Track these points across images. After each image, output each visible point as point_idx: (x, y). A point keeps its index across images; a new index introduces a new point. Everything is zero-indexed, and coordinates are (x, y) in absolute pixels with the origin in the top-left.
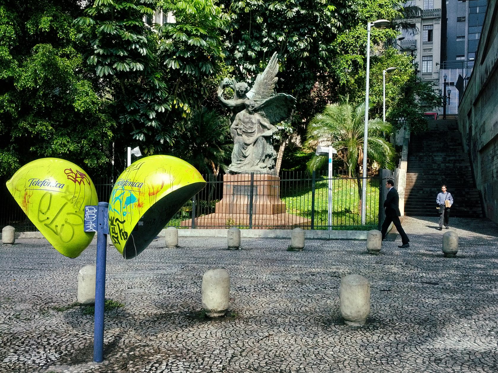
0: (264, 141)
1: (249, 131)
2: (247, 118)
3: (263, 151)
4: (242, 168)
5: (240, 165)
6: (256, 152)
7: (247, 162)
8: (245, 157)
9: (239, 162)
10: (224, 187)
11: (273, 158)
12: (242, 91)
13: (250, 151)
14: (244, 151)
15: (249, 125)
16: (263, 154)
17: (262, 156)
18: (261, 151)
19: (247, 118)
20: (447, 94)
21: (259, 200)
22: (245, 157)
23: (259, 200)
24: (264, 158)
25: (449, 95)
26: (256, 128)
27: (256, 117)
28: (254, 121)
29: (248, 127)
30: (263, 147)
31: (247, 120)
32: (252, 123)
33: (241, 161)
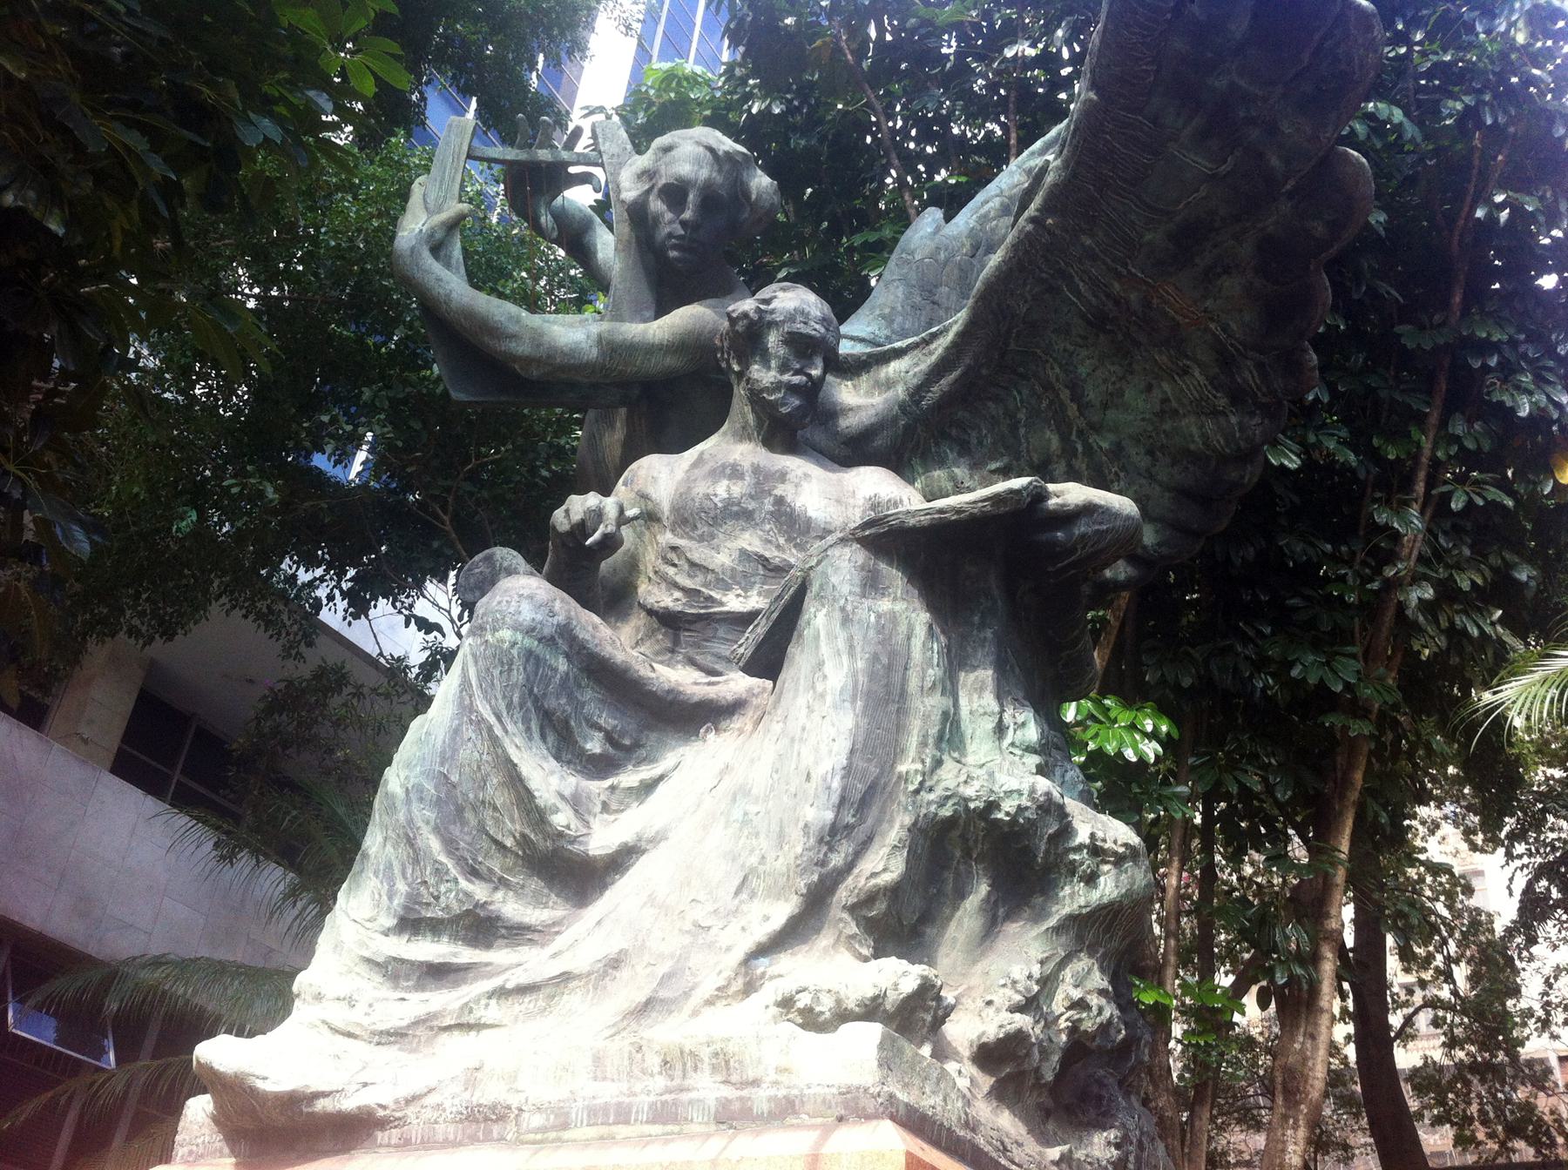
0: (906, 612)
11: (1074, 898)
22: (577, 876)
30: (884, 697)
33: (481, 927)
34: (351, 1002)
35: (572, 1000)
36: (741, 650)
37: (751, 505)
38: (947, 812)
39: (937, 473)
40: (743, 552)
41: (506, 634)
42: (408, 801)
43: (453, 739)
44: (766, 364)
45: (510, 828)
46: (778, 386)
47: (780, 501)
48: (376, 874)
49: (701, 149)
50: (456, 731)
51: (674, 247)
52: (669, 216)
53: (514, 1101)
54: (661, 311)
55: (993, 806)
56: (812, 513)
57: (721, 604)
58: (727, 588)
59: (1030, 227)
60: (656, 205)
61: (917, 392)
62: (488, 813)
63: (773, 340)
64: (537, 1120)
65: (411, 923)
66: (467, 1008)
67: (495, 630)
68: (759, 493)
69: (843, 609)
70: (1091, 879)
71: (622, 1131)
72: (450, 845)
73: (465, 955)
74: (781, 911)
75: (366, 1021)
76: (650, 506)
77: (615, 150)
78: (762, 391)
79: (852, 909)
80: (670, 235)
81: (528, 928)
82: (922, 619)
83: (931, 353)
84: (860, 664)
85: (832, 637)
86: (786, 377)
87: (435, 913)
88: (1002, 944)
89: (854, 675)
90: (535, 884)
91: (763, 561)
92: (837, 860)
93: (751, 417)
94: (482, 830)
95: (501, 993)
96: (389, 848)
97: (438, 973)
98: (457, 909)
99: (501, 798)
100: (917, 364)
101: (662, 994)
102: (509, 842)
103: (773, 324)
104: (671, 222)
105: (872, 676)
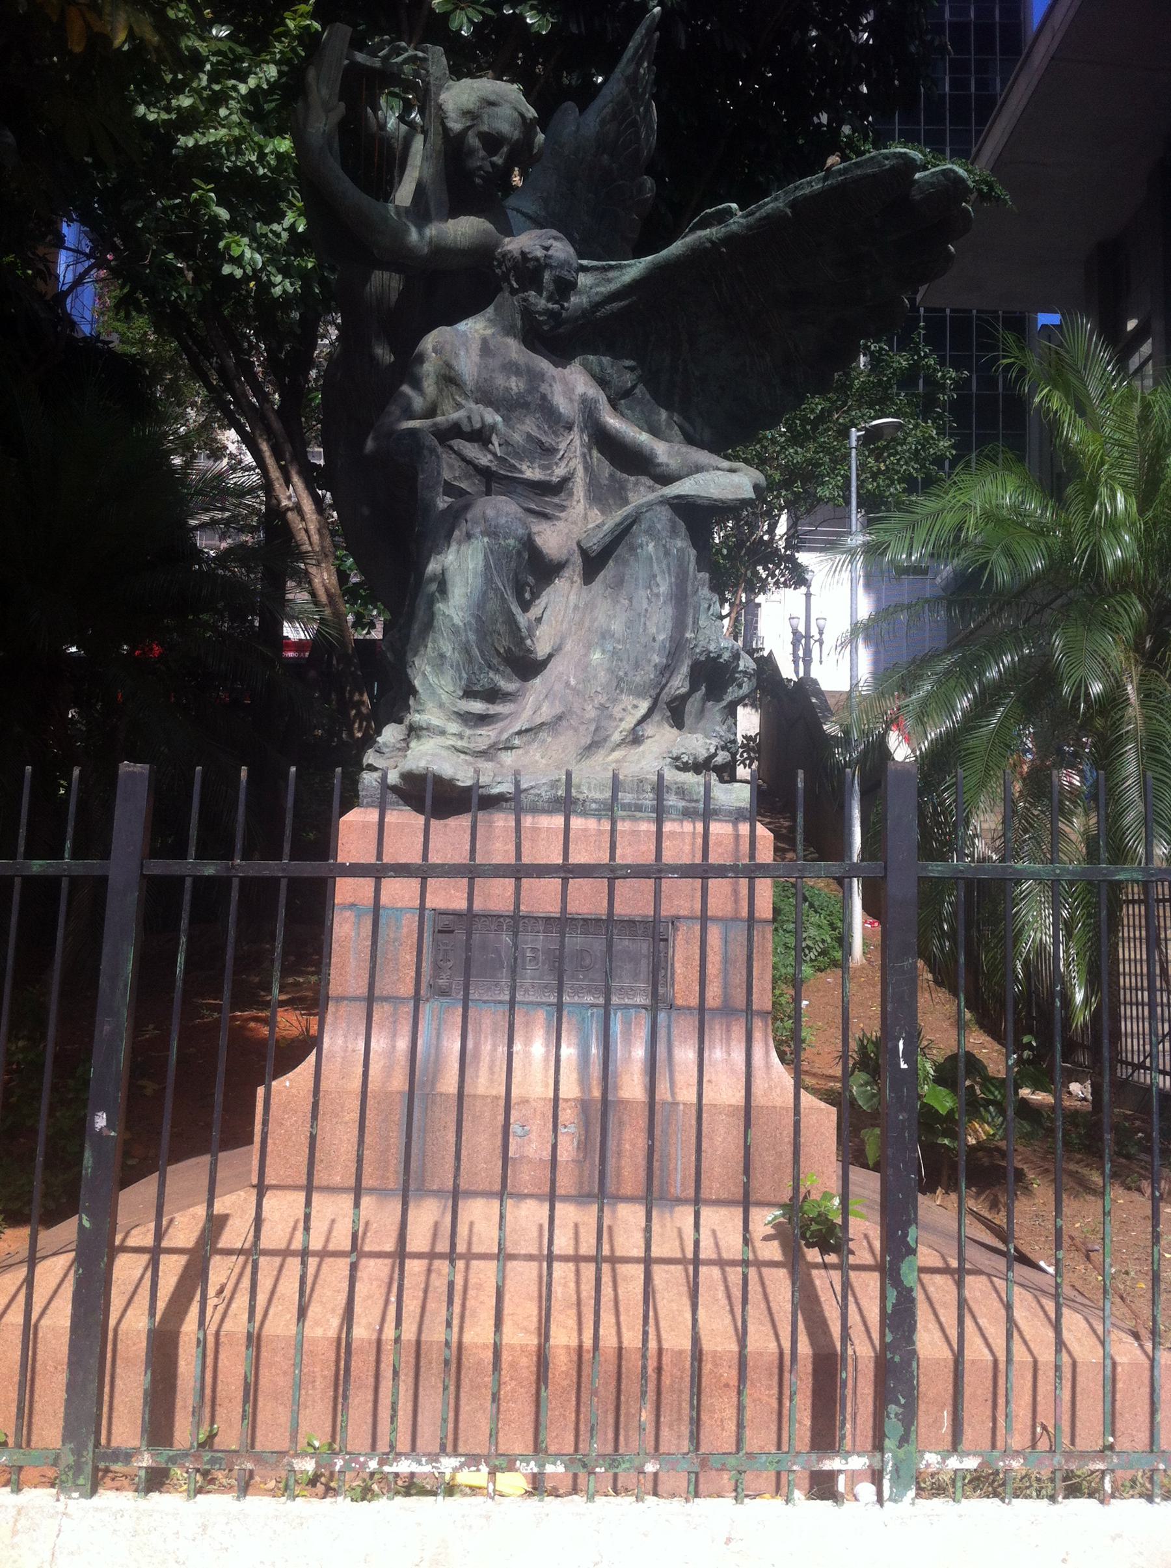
1: (531, 472)
2: (512, 368)
3: (679, 625)
4: (508, 758)
5: (486, 735)
6: (617, 626)
7: (546, 713)
8: (527, 666)
9: (477, 707)
10: (347, 932)
12: (492, 141)
13: (561, 616)
14: (522, 619)
15: (529, 426)
16: (676, 648)
17: (667, 670)
18: (658, 623)
19: (512, 368)
20: (814, 631)
21: (686, 1055)
22: (527, 666)
23: (686, 1055)
24: (679, 684)
25: (821, 633)
26: (573, 456)
27: (572, 385)
28: (563, 405)
29: (517, 438)
31: (516, 385)
32: (549, 414)
33: (493, 695)
34: (461, 736)
35: (543, 735)
36: (595, 547)
37: (529, 399)
38: (703, 658)
39: (591, 357)
40: (529, 435)
41: (511, 542)
42: (466, 631)
43: (483, 596)
44: (540, 293)
45: (503, 644)
46: (547, 312)
47: (544, 397)
48: (452, 666)
49: (516, 114)
50: (484, 594)
51: (480, 177)
52: (482, 153)
53: (581, 797)
54: (454, 213)
55: (720, 656)
56: (562, 410)
57: (521, 472)
58: (521, 460)
59: (708, 245)
60: (473, 141)
61: (596, 306)
62: (495, 636)
63: (547, 276)
64: (594, 806)
65: (469, 694)
66: (508, 740)
67: (505, 538)
68: (533, 389)
69: (664, 546)
70: (740, 686)
71: (638, 814)
72: (481, 652)
73: (494, 709)
74: (644, 706)
75: (471, 746)
76: (453, 374)
77: (439, 74)
78: (537, 312)
79: (668, 704)
80: (480, 168)
81: (510, 694)
82: (693, 553)
83: (609, 281)
84: (673, 580)
85: (659, 562)
86: (550, 306)
87: (477, 688)
88: (707, 714)
89: (671, 583)
90: (508, 670)
91: (540, 443)
92: (664, 681)
93: (519, 323)
94: (493, 645)
95: (519, 733)
96: (456, 654)
97: (483, 719)
98: (487, 686)
99: (501, 627)
100: (597, 285)
101: (596, 739)
102: (502, 651)
103: (548, 266)
104: (483, 159)
105: (677, 585)
